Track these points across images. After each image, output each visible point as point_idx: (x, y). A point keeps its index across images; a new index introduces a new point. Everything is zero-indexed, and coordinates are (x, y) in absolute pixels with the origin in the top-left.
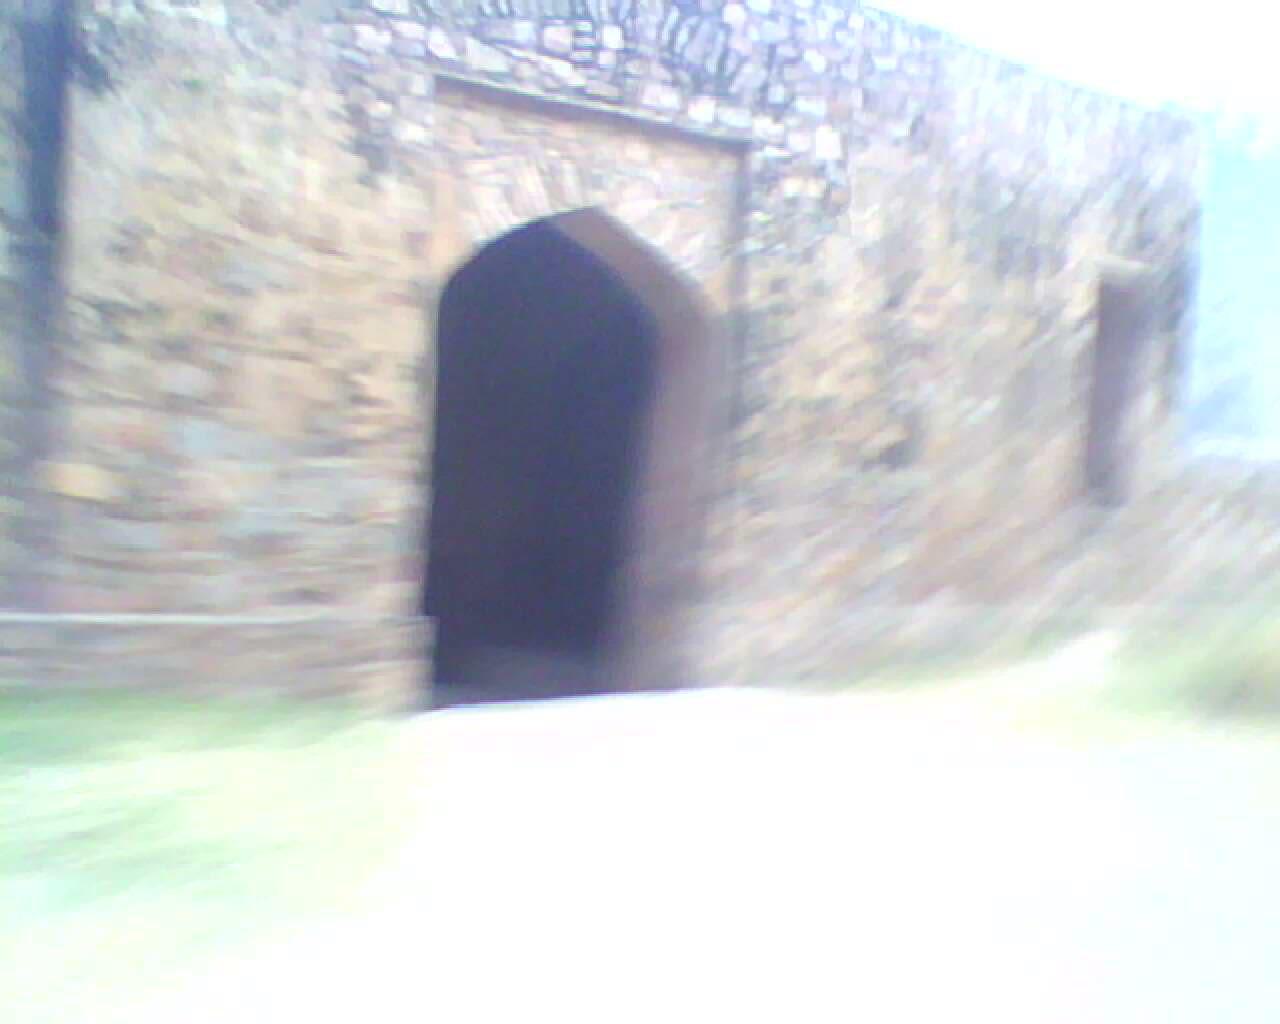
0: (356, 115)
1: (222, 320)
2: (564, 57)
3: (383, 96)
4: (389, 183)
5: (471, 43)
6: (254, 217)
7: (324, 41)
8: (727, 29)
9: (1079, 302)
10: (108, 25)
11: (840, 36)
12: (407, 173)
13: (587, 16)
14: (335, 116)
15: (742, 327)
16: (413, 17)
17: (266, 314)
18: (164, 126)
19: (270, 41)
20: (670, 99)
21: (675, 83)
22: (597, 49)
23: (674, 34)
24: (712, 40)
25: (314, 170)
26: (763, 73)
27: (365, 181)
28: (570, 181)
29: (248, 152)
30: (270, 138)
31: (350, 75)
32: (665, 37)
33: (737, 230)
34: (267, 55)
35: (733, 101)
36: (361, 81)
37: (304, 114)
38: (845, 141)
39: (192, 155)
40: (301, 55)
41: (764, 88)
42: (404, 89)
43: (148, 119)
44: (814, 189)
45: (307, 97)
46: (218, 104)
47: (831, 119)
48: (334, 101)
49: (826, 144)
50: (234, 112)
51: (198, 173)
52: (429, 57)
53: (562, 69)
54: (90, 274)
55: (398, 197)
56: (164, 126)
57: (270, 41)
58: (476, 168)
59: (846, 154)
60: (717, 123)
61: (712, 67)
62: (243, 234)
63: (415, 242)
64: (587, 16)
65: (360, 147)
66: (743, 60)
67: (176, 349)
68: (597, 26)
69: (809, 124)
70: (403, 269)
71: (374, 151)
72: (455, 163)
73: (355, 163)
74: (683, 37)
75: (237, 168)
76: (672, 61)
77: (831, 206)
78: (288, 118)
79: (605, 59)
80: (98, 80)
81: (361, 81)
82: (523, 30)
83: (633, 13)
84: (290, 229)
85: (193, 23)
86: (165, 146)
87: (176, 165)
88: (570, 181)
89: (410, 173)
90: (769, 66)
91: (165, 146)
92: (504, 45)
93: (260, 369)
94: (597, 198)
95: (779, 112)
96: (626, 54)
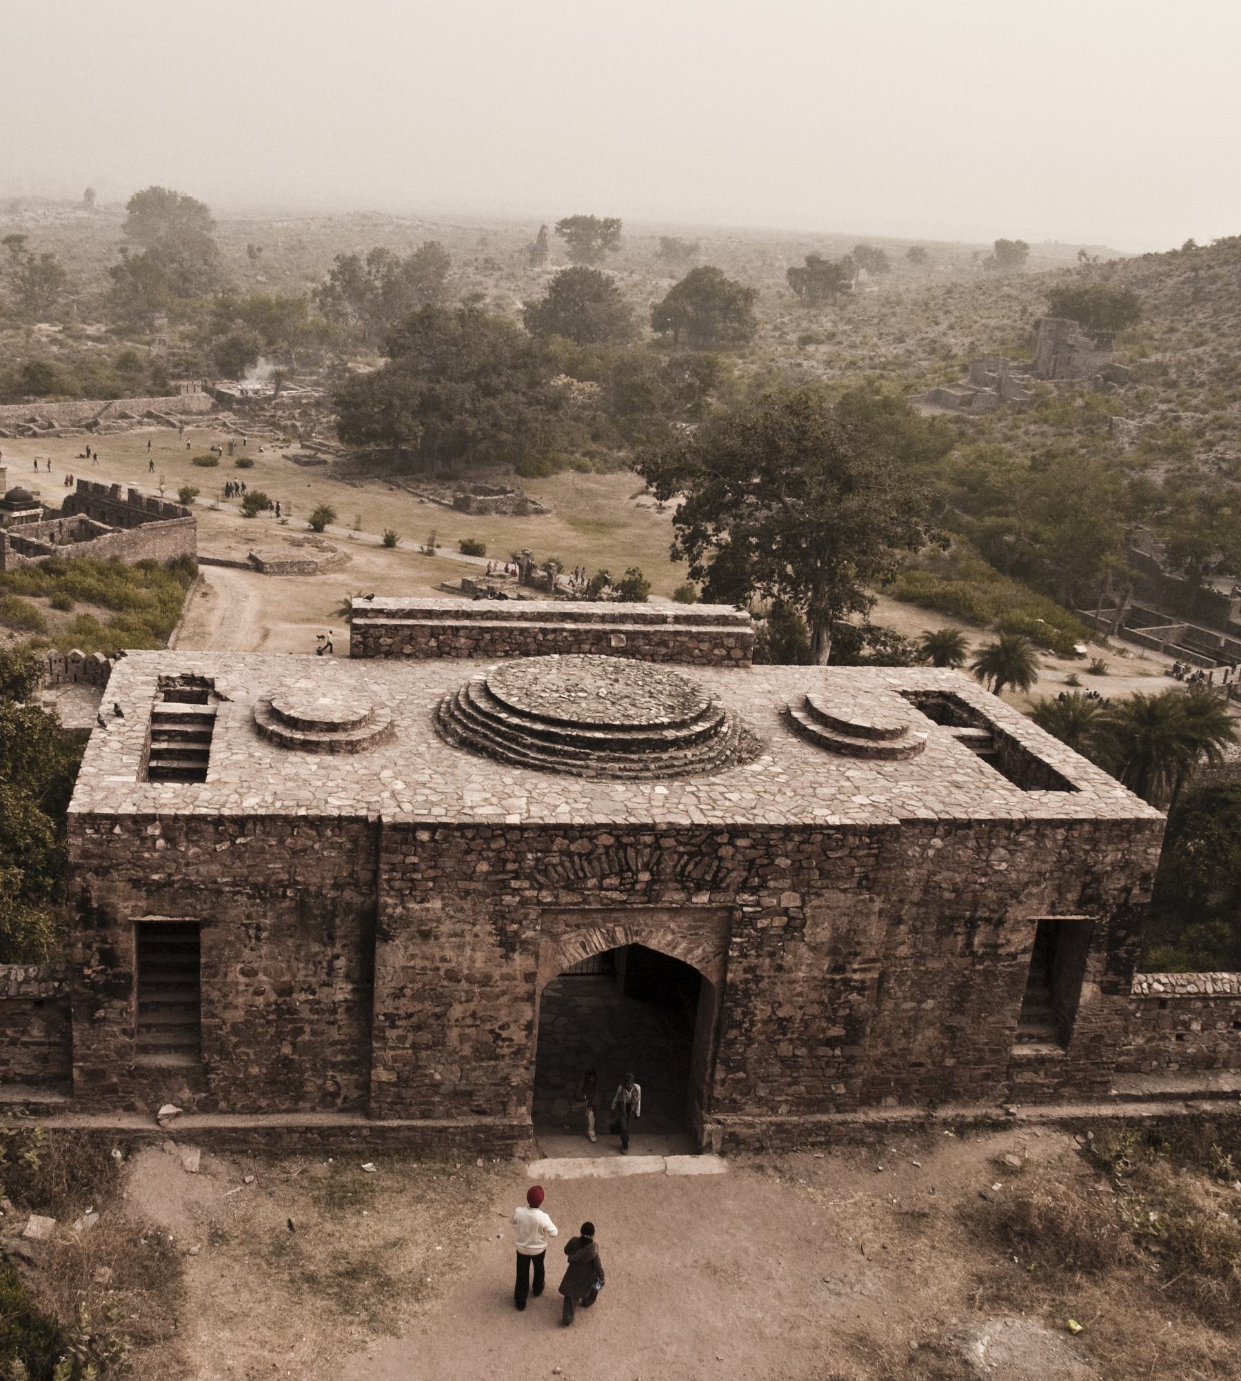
0: (501, 931)
1: (438, 1016)
2: (616, 889)
3: (513, 922)
4: (516, 956)
5: (562, 893)
6: (452, 976)
7: (487, 904)
8: (721, 859)
9: (1021, 939)
10: (391, 917)
11: (802, 847)
12: (525, 950)
13: (629, 869)
14: (490, 934)
15: (726, 988)
16: (532, 887)
17: (457, 1011)
18: (412, 950)
19: (462, 910)
20: (679, 896)
21: (684, 888)
22: (633, 884)
23: (684, 868)
24: (710, 866)
25: (480, 956)
26: (745, 874)
27: (506, 957)
28: (620, 935)
29: (449, 953)
30: (461, 947)
31: (499, 917)
32: (678, 869)
33: (725, 945)
34: (459, 915)
35: (726, 890)
36: (504, 918)
37: (476, 935)
38: (803, 896)
39: (425, 958)
40: (475, 913)
41: (746, 880)
42: (526, 916)
43: (406, 948)
44: (780, 921)
45: (478, 928)
46: (437, 938)
47: (793, 888)
48: (489, 928)
49: (790, 900)
50: (443, 939)
51: (427, 964)
52: (539, 903)
53: (615, 895)
54: (383, 1006)
55: (520, 962)
56: (412, 950)
57: (462, 910)
58: (566, 937)
59: (803, 901)
60: (710, 901)
61: (708, 878)
62: (445, 983)
63: (530, 977)
64: (629, 869)
65: (501, 945)
66: (729, 871)
67: (418, 1028)
68: (635, 873)
69: (778, 892)
70: (523, 988)
71: (509, 944)
72: (555, 937)
73: (499, 951)
74: (690, 867)
75: (444, 959)
76: (681, 879)
77: (794, 926)
78: (468, 938)
79: (638, 887)
80: (387, 938)
81: (504, 918)
82: (592, 882)
83: (658, 863)
84: (469, 979)
85: (428, 909)
86: (413, 956)
87: (418, 963)
88: (620, 935)
89: (526, 950)
90: (749, 871)
91: (413, 956)
92: (580, 891)
93: (454, 1034)
94: (637, 939)
95: (754, 891)
96: (653, 881)
